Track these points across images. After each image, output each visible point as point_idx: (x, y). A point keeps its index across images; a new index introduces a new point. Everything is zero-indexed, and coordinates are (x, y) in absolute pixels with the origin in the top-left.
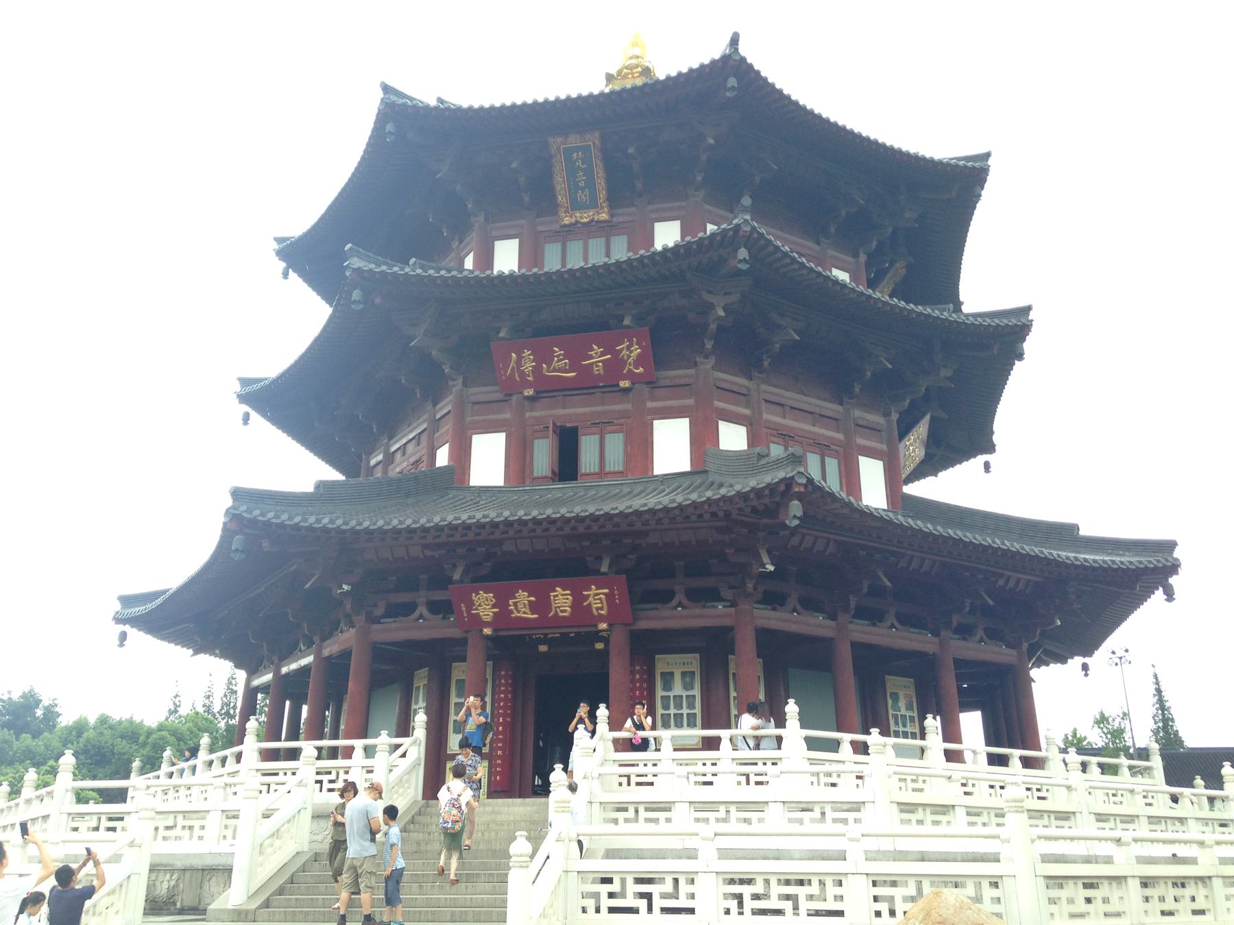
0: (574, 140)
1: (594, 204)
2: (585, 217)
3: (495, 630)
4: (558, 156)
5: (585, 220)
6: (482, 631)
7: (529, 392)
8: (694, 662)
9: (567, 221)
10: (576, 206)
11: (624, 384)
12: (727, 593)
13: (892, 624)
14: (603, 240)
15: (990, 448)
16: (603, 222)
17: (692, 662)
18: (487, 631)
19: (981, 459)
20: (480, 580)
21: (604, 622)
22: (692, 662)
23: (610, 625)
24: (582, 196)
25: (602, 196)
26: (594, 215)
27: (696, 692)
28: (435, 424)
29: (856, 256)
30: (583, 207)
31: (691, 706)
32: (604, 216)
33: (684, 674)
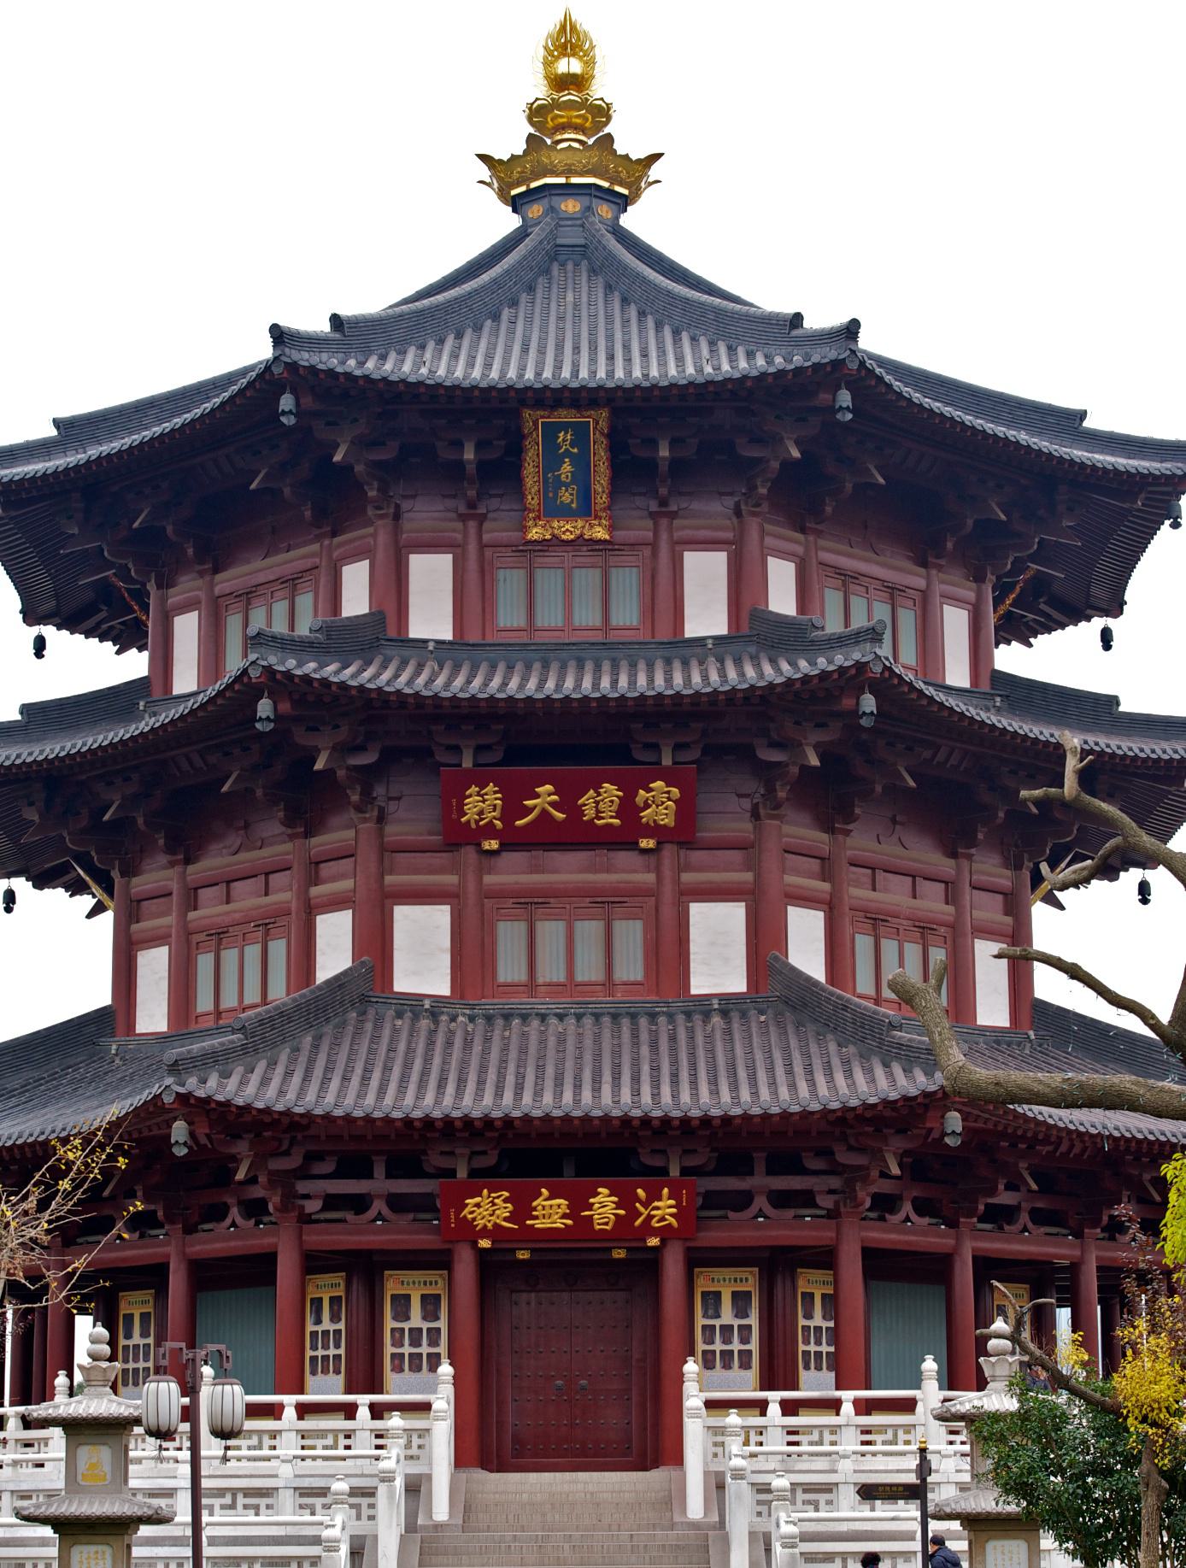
0: (565, 416)
1: (585, 509)
2: (568, 529)
3: (493, 1242)
4: (535, 436)
5: (564, 537)
6: (476, 1243)
7: (494, 845)
8: (750, 1277)
9: (535, 533)
10: (553, 510)
11: (646, 843)
12: (826, 1202)
13: (1025, 1227)
14: (598, 572)
15: (1115, 607)
16: (600, 542)
17: (749, 1281)
18: (485, 1243)
19: (1098, 623)
20: (484, 1178)
21: (656, 1236)
22: (749, 1281)
23: (663, 1241)
24: (566, 496)
25: (602, 499)
26: (583, 527)
27: (753, 1320)
28: (313, 871)
29: (979, 579)
30: (565, 513)
31: (745, 1340)
32: (600, 533)
33: (735, 1295)
